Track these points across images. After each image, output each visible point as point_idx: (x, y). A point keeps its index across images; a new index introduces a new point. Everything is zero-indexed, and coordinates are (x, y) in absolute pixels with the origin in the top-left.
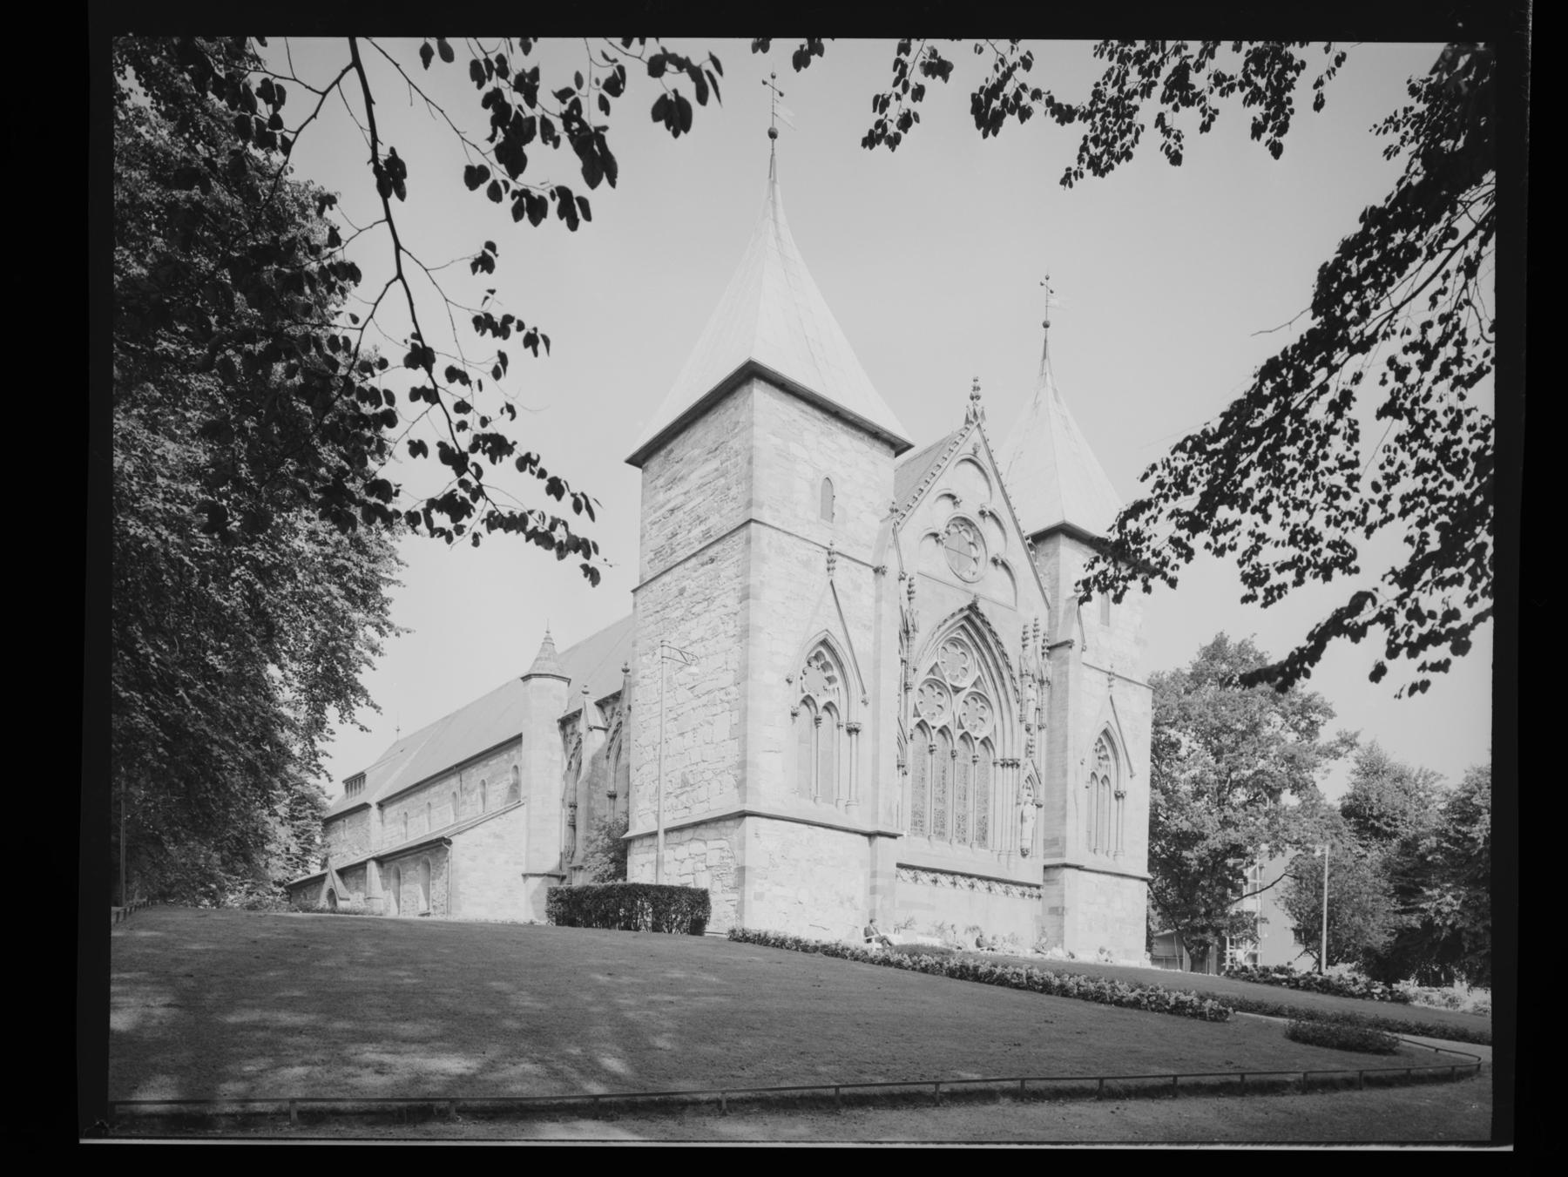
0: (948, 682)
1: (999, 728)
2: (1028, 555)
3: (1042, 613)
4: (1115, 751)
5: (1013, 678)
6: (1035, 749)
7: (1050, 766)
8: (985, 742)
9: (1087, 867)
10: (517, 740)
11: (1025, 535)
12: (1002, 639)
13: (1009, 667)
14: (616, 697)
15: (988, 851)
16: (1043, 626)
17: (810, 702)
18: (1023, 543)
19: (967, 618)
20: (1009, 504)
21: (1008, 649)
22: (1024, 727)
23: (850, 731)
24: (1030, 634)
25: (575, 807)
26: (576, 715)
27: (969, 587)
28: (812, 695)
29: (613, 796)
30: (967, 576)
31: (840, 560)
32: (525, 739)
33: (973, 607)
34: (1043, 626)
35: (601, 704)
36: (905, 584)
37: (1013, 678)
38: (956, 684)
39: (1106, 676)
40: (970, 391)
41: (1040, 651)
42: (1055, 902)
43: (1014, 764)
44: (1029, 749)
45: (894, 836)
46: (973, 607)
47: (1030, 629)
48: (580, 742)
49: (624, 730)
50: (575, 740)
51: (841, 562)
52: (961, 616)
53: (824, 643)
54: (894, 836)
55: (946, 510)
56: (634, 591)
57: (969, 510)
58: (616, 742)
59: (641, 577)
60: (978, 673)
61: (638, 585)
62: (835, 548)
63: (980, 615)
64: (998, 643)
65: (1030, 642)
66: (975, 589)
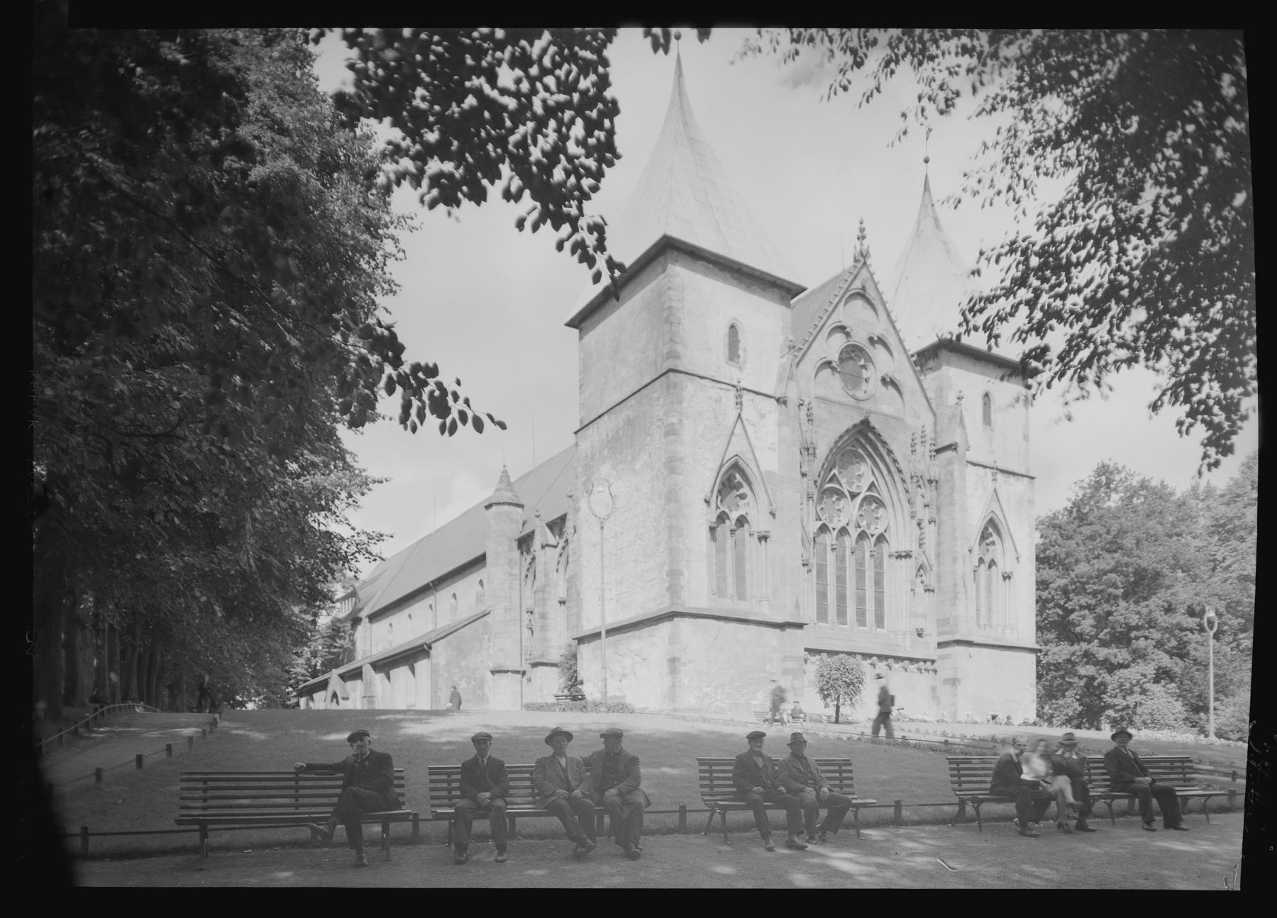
0: (845, 489)
1: (892, 525)
2: (915, 371)
3: (928, 419)
5: (904, 481)
6: (926, 541)
7: (938, 555)
8: (881, 538)
9: (977, 640)
10: (480, 561)
11: (910, 353)
12: (893, 446)
13: (900, 471)
14: (563, 519)
17: (724, 517)
18: (909, 359)
19: (860, 432)
20: (894, 328)
21: (898, 455)
22: (915, 522)
23: (760, 539)
24: (918, 441)
25: (532, 613)
26: (530, 536)
28: (727, 510)
29: (562, 603)
30: (860, 395)
31: (747, 397)
32: (489, 559)
33: (865, 422)
35: (551, 526)
36: (804, 409)
37: (904, 481)
40: (857, 233)
41: (928, 454)
42: (949, 675)
45: (800, 626)
46: (865, 422)
47: (918, 435)
48: (534, 559)
49: (571, 546)
50: (529, 558)
51: (747, 397)
52: (851, 433)
53: (736, 467)
54: (800, 626)
55: (839, 341)
56: (576, 433)
57: (860, 338)
58: (564, 556)
59: (581, 422)
60: (873, 479)
61: (578, 427)
62: (743, 385)
63: (872, 429)
64: (890, 452)
65: (918, 447)
66: (867, 406)
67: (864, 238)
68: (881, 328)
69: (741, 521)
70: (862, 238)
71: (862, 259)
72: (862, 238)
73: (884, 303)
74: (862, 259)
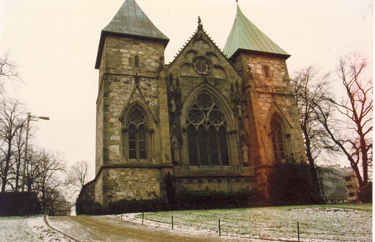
4: (282, 120)
5: (228, 102)
13: (226, 99)
15: (229, 166)
16: (240, 82)
27: (205, 77)
30: (205, 73)
34: (240, 82)
38: (207, 109)
39: (270, 96)
41: (240, 92)
43: (235, 132)
44: (241, 126)
57: (202, 53)
67: (200, 22)
68: (212, 50)
69: (141, 126)
70: (199, 22)
71: (200, 27)
72: (199, 22)
73: (211, 41)
74: (200, 27)
